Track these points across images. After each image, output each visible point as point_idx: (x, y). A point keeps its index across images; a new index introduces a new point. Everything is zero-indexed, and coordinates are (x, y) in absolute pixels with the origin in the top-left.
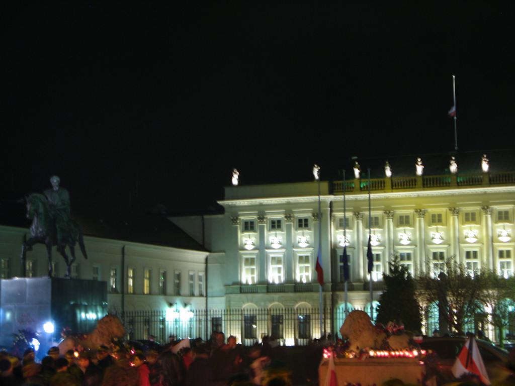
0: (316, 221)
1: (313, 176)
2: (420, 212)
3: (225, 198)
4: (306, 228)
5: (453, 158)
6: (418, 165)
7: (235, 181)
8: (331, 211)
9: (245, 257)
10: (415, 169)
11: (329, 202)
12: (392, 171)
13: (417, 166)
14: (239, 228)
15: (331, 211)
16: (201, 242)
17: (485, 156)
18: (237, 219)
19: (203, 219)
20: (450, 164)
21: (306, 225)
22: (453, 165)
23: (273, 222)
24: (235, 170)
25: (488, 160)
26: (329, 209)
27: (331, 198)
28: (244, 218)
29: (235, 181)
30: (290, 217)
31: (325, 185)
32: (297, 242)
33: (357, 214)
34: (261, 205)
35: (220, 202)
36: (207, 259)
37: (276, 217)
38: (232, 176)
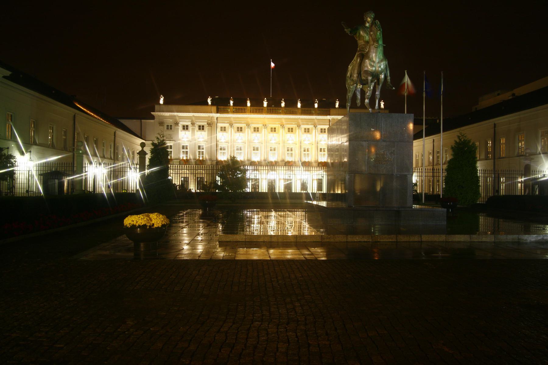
0: (209, 127)
2: (265, 126)
3: (155, 111)
4: (203, 130)
5: (283, 99)
7: (161, 102)
10: (263, 104)
12: (251, 102)
13: (264, 102)
15: (217, 122)
16: (140, 135)
17: (299, 100)
19: (141, 122)
20: (281, 103)
21: (203, 129)
22: (283, 103)
23: (184, 126)
24: (161, 96)
27: (218, 115)
29: (161, 102)
30: (194, 124)
31: (214, 108)
33: (231, 125)
35: (152, 113)
38: (159, 99)
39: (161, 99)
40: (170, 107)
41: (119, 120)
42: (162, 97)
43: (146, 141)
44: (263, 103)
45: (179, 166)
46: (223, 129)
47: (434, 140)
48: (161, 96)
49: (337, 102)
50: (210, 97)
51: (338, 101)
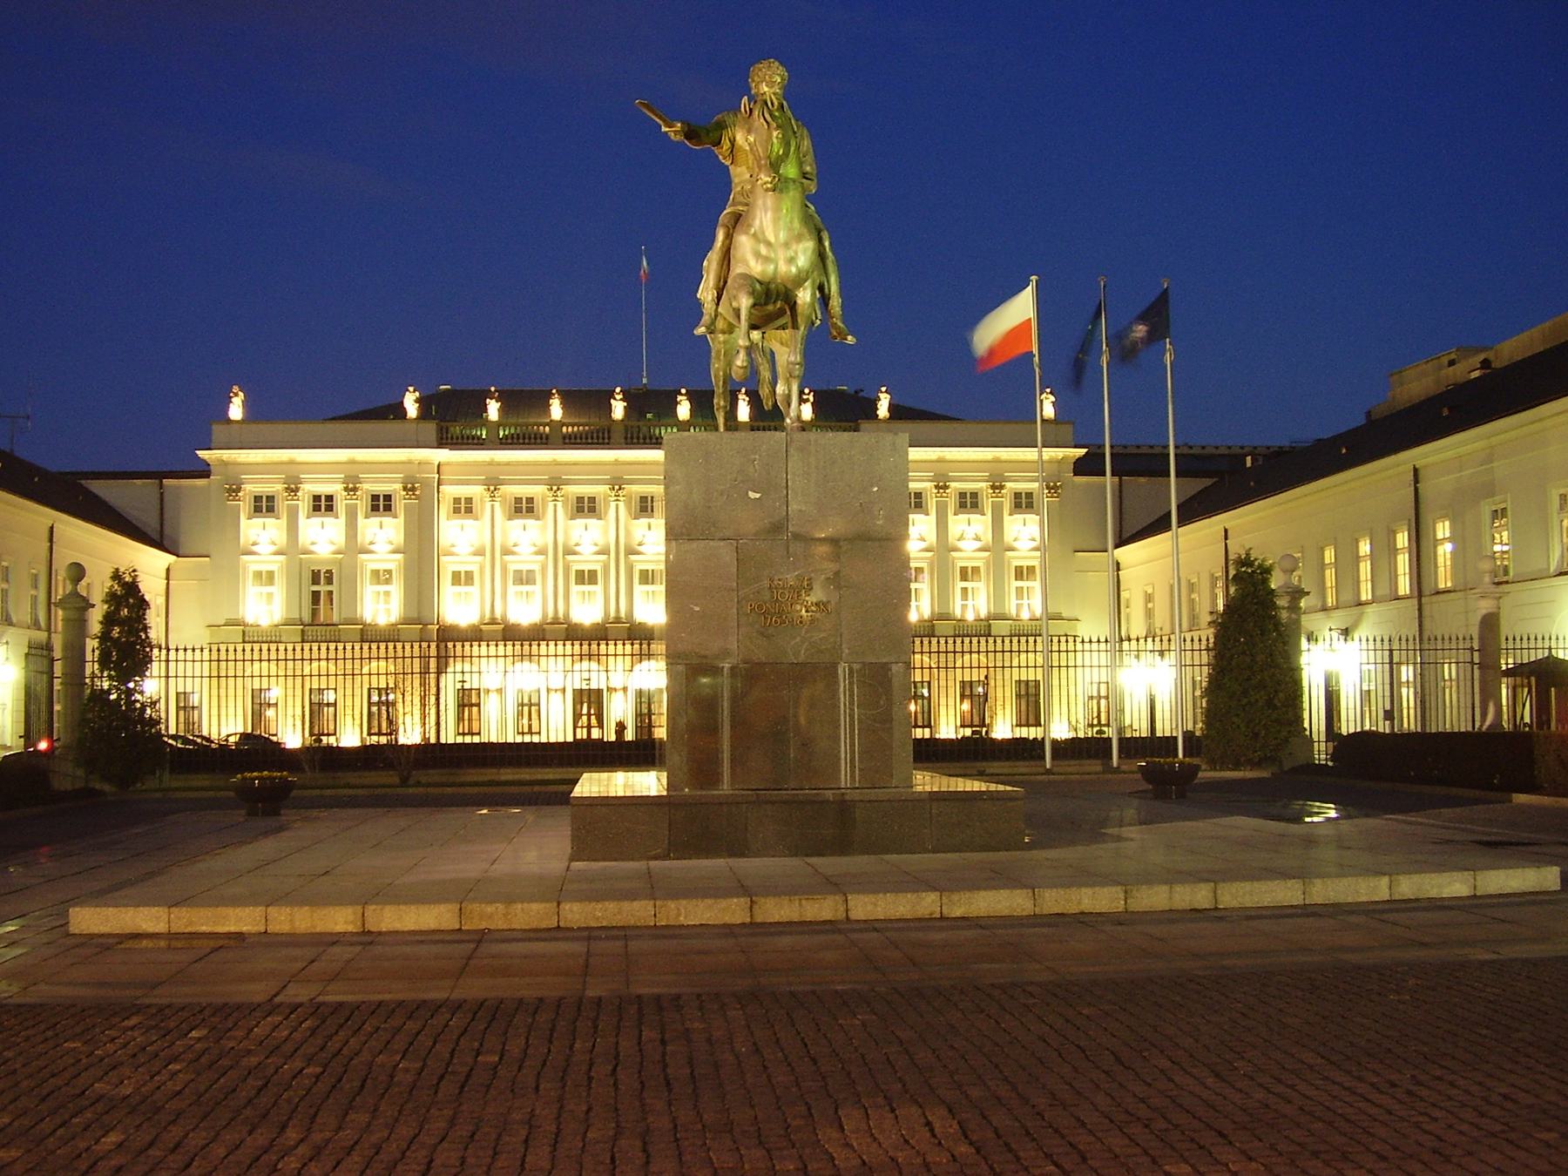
1: (404, 412)
6: (615, 399)
8: (439, 485)
9: (253, 568)
11: (436, 464)
12: (565, 405)
13: (612, 401)
14: (245, 506)
16: (156, 536)
17: (743, 390)
18: (239, 490)
20: (677, 403)
24: (235, 389)
25: (747, 399)
26: (437, 476)
28: (251, 488)
29: (236, 411)
30: (355, 489)
31: (431, 428)
32: (368, 542)
34: (292, 463)
35: (201, 454)
36: (168, 570)
37: (323, 489)
39: (233, 400)
40: (265, 429)
41: (83, 482)
42: (236, 395)
43: (178, 556)
44: (611, 405)
45: (298, 648)
46: (464, 508)
47: (1226, 531)
48: (235, 389)
49: (882, 396)
50: (411, 389)
51: (886, 392)
